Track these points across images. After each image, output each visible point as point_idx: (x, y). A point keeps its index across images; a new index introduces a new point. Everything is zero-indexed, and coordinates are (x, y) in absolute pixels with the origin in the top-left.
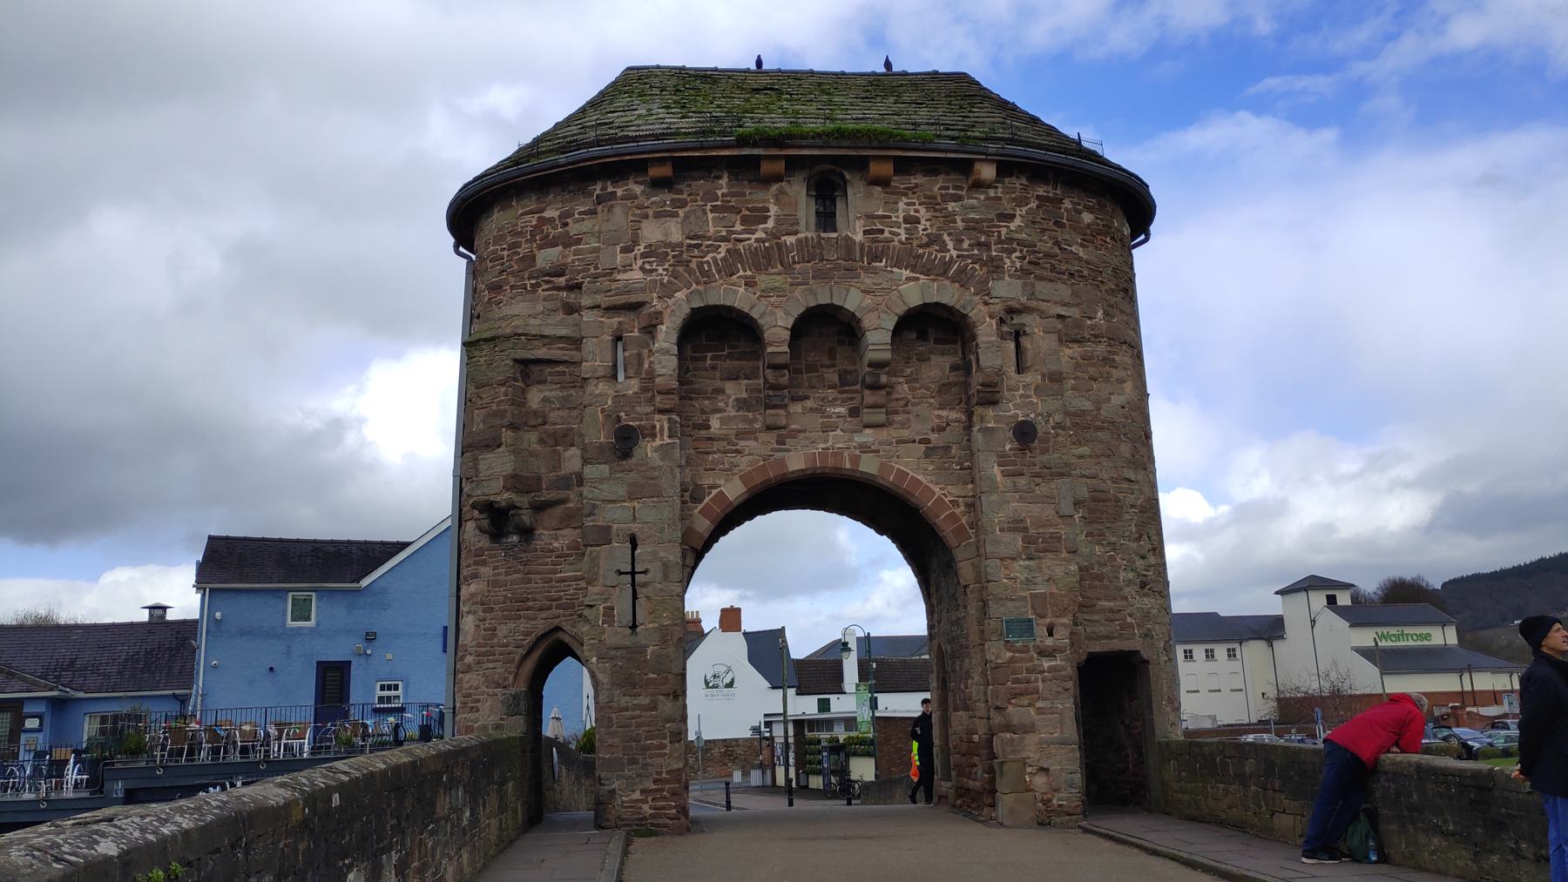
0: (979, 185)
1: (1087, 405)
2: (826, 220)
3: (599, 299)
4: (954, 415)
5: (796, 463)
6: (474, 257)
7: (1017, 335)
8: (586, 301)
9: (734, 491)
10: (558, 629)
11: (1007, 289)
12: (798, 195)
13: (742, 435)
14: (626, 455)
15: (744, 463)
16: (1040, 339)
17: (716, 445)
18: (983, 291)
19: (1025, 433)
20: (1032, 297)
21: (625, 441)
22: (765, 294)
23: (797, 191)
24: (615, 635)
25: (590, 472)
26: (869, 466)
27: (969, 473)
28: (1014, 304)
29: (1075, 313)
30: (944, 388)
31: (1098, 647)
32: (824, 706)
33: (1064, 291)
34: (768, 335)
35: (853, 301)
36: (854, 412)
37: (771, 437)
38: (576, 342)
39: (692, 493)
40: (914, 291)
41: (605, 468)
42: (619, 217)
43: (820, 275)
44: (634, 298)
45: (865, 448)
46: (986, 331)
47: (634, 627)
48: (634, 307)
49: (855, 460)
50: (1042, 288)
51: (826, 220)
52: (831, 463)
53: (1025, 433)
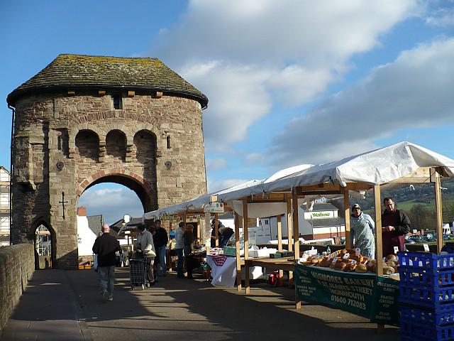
1: (186, 157)
3: (53, 127)
4: (150, 159)
5: (107, 172)
6: (15, 109)
9: (90, 180)
10: (42, 217)
11: (165, 126)
12: (109, 100)
15: (94, 172)
16: (173, 140)
17: (85, 167)
18: (159, 127)
19: (168, 165)
20: (172, 127)
21: (59, 166)
23: (109, 97)
26: (127, 173)
28: (166, 130)
29: (183, 132)
30: (148, 151)
34: (100, 137)
35: (123, 128)
40: (140, 127)
41: (55, 174)
44: (63, 127)
45: (126, 168)
46: (158, 137)
47: (64, 217)
49: (123, 171)
52: (117, 172)
53: (168, 165)
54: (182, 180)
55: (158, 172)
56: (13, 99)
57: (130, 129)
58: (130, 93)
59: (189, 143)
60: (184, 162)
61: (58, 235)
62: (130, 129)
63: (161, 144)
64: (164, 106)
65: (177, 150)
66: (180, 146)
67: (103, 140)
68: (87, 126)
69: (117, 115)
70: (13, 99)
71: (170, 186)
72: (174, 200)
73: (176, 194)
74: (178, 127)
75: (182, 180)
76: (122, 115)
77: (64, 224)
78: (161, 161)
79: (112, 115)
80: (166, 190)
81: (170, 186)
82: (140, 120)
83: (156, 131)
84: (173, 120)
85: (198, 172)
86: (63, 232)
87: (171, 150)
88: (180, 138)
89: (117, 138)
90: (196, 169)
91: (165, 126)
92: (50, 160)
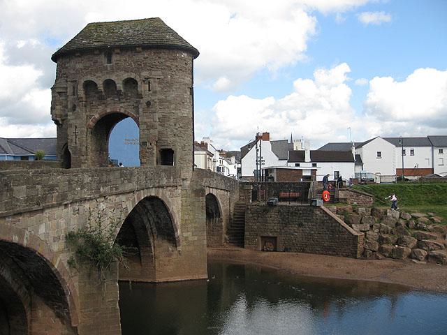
0: (139, 52)
2: (109, 61)
7: (149, 83)
8: (69, 80)
11: (145, 74)
13: (99, 105)
14: (75, 110)
19: (148, 104)
21: (74, 108)
22: (97, 78)
23: (103, 56)
24: (73, 145)
25: (69, 113)
27: (138, 112)
29: (162, 77)
31: (162, 148)
32: (298, 165)
33: (160, 73)
35: (113, 78)
36: (119, 100)
37: (104, 105)
38: (66, 88)
39: (89, 117)
40: (126, 76)
41: (71, 113)
42: (72, 64)
43: (107, 73)
45: (121, 107)
46: (139, 83)
48: (76, 81)
50: (153, 73)
51: (109, 61)
52: (115, 110)
53: (148, 104)
54: (157, 116)
55: (141, 110)
56: (55, 58)
57: (119, 79)
58: (96, 52)
59: (167, 85)
60: (161, 101)
61: (72, 156)
62: (119, 79)
63: (143, 88)
64: (144, 58)
65: (155, 92)
66: (158, 89)
67: (101, 87)
68: (90, 78)
69: (109, 68)
70: (55, 58)
71: (149, 120)
72: (152, 131)
73: (153, 127)
74: (158, 74)
75: (157, 116)
76: (112, 67)
77: (76, 147)
78: (144, 101)
79: (106, 68)
80: (145, 123)
81: (149, 120)
82: (126, 71)
83: (138, 79)
84: (152, 68)
85: (175, 109)
86: (75, 153)
87: (151, 92)
88: (159, 83)
89: (109, 84)
90: (173, 106)
91: (145, 74)
92: (69, 103)
